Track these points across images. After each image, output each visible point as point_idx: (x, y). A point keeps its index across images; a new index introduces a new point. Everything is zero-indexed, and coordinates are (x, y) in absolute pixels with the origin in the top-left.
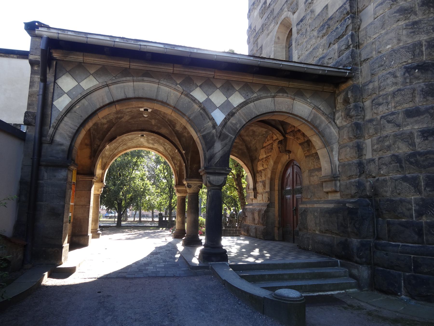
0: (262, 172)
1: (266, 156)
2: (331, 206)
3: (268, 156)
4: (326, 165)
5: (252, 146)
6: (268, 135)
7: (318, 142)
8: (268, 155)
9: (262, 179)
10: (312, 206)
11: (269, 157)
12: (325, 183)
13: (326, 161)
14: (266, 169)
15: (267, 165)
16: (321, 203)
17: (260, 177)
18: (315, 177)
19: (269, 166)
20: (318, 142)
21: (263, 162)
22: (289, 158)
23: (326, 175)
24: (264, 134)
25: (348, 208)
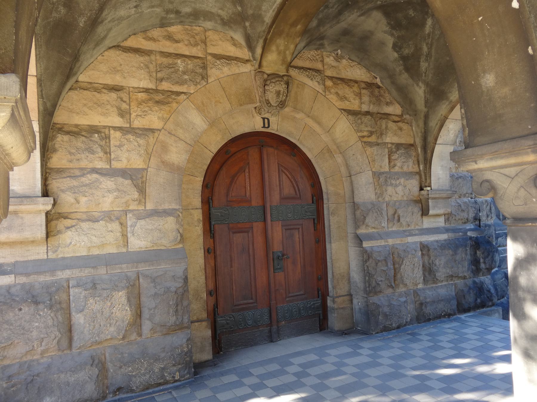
0: (108, 137)
1: (151, 86)
2: (443, 237)
3: (178, 94)
4: (441, 172)
5: (109, 19)
6: (181, 22)
7: (452, 132)
8: (165, 86)
9: (109, 161)
10: (402, 241)
11: (183, 97)
12: (433, 200)
13: (442, 166)
14: (152, 131)
15: (166, 121)
16: (415, 235)
17: (101, 154)
18: (400, 189)
19: (170, 126)
20: (452, 132)
21: (122, 100)
22: (264, 127)
23: (440, 188)
24: (178, 12)
25: (471, 238)
